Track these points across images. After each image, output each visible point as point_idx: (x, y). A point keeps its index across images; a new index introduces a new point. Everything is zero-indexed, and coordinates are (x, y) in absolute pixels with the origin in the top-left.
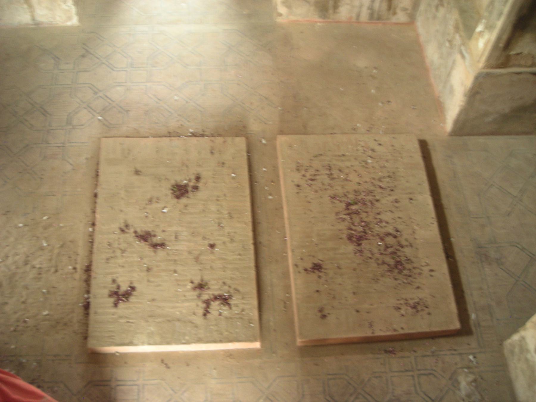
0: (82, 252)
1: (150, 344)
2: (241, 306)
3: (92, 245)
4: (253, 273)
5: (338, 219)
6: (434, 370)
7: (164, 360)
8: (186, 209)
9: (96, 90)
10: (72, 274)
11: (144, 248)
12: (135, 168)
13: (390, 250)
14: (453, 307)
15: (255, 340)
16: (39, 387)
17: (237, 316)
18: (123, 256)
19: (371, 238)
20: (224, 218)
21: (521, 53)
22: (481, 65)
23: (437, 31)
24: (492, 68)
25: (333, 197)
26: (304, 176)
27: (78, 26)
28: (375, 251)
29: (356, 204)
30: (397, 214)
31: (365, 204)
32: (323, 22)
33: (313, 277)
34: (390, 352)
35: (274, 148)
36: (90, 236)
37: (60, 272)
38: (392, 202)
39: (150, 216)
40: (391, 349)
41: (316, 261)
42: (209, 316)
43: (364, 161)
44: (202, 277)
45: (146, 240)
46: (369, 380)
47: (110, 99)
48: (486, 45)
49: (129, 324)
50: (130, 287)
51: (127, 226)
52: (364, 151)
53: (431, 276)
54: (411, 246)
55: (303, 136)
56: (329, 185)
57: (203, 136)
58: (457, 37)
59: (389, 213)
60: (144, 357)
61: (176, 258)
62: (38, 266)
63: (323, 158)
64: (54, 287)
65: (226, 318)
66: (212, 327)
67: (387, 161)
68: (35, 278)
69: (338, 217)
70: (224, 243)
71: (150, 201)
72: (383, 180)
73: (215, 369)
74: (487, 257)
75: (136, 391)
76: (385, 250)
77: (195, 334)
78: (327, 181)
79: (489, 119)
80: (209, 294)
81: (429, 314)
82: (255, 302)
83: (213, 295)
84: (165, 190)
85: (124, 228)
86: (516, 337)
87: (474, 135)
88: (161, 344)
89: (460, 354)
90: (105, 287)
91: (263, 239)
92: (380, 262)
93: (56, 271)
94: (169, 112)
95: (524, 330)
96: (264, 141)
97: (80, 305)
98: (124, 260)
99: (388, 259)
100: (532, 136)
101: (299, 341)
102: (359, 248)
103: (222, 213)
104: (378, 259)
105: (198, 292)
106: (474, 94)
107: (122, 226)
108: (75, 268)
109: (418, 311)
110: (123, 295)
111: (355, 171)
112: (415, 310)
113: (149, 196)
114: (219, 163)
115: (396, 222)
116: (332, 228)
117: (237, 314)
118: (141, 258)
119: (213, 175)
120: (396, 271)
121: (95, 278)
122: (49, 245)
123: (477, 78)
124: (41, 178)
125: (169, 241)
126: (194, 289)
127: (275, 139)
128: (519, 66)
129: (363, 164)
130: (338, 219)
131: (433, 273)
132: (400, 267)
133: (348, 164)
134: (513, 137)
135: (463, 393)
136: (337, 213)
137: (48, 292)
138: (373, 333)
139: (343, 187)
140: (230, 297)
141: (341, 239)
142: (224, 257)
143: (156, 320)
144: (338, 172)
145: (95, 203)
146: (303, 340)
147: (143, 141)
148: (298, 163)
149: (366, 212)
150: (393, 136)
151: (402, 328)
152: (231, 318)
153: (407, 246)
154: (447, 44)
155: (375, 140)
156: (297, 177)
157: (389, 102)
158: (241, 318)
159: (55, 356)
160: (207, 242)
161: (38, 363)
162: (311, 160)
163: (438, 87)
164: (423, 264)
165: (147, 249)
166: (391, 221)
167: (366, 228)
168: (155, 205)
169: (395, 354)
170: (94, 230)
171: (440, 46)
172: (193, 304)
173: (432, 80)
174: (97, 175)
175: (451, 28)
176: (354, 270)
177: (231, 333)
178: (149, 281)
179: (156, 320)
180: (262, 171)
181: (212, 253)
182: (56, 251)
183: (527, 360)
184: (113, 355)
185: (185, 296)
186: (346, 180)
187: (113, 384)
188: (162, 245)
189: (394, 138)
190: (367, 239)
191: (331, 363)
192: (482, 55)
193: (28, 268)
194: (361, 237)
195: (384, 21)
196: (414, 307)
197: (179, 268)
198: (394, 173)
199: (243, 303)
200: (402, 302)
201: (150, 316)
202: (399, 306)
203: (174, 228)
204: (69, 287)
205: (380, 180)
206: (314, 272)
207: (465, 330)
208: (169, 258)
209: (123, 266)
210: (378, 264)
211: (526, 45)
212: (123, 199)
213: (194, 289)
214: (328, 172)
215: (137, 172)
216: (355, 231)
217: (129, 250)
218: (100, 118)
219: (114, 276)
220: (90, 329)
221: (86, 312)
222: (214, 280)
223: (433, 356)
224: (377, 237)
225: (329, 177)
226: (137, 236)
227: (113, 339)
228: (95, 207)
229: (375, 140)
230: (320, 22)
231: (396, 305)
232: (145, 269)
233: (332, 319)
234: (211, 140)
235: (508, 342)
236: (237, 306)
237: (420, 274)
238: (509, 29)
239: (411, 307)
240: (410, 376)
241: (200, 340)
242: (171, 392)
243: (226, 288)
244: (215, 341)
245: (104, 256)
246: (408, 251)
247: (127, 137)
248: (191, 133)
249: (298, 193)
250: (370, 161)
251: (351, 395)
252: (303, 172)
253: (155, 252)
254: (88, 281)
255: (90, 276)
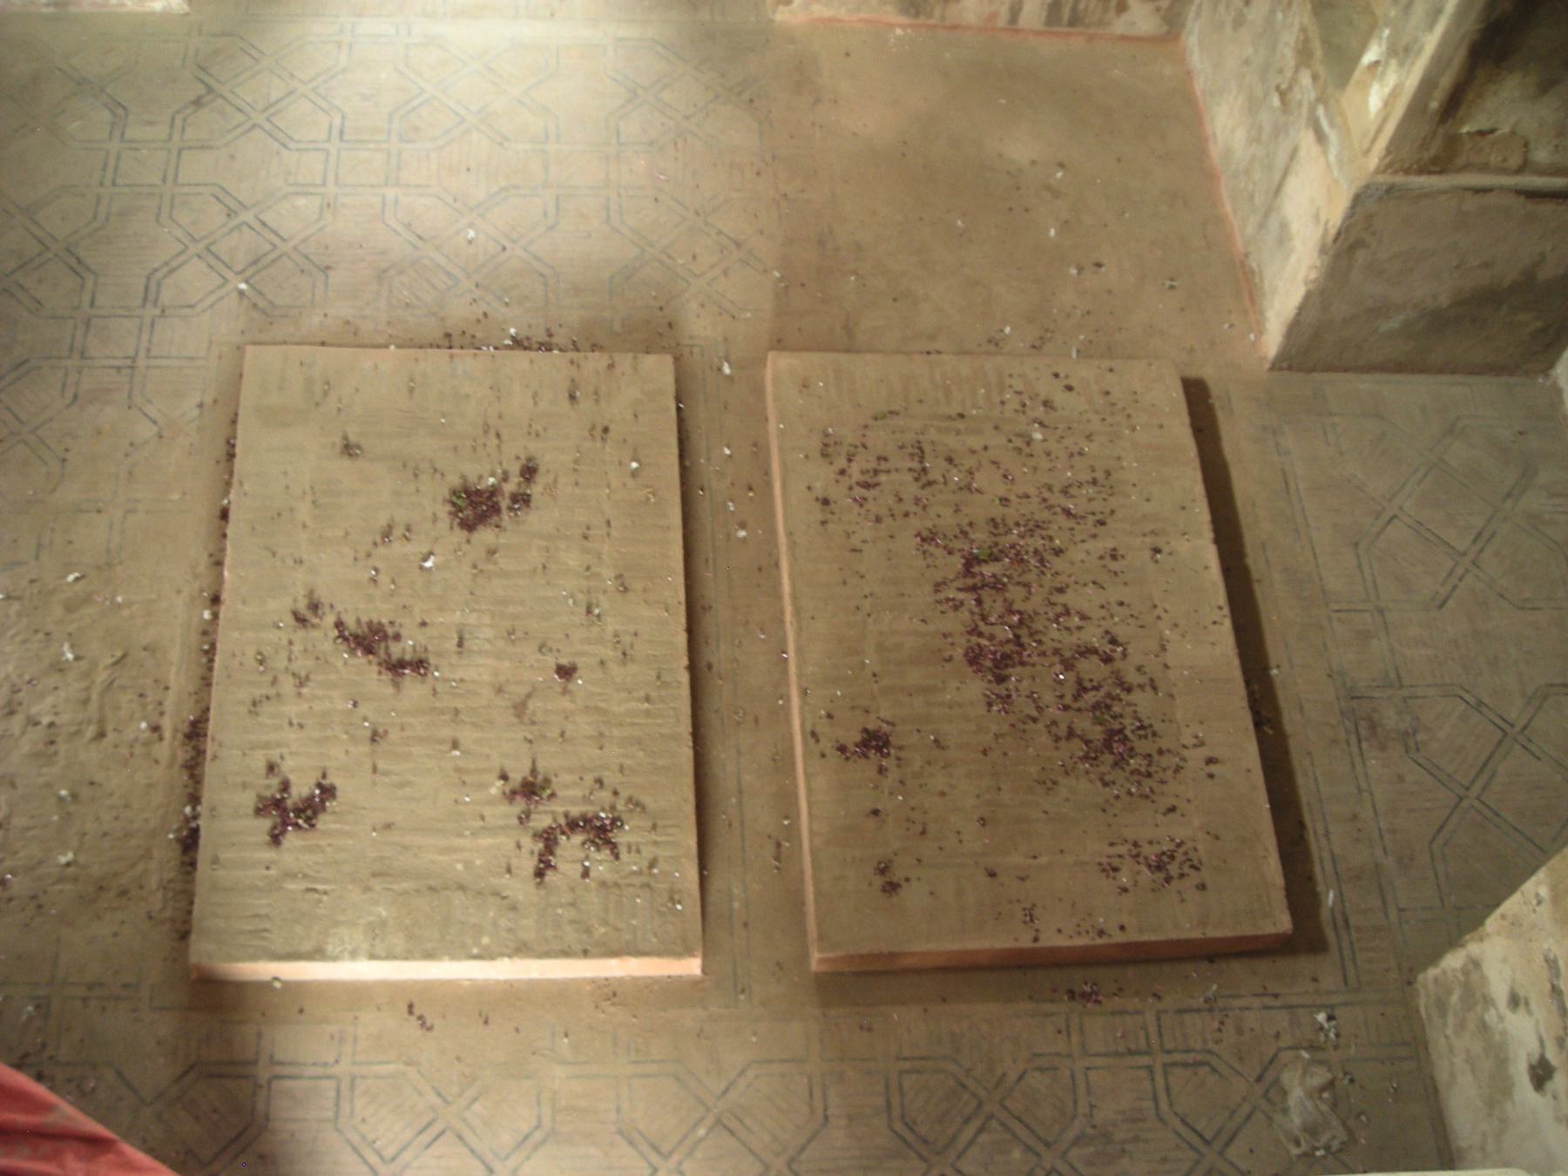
0: (178, 676)
1: (373, 956)
2: (648, 853)
3: (211, 660)
4: (686, 753)
5: (940, 602)
6: (1210, 1052)
7: (415, 1005)
8: (495, 563)
9: (232, 204)
10: (147, 744)
11: (366, 672)
12: (345, 438)
13: (1090, 698)
14: (1273, 866)
15: (688, 952)
16: (39, 1077)
17: (637, 881)
18: (299, 694)
19: (1035, 659)
20: (605, 592)
21: (1492, 131)
22: (1373, 162)
23: (1247, 62)
24: (1407, 172)
25: (928, 538)
26: (842, 472)
27: (187, 14)
28: (1048, 698)
29: (997, 560)
30: (1114, 593)
31: (1019, 560)
32: (914, 27)
33: (863, 769)
34: (1084, 996)
35: (758, 391)
36: (205, 633)
37: (111, 736)
38: (1101, 558)
39: (384, 579)
40: (1088, 989)
41: (870, 727)
42: (550, 876)
43: (1019, 435)
44: (534, 763)
45: (369, 651)
46: (1021, 1078)
47: (276, 233)
48: (1388, 103)
49: (309, 896)
50: (319, 785)
51: (315, 607)
52: (1024, 405)
53: (1211, 776)
54: (1155, 688)
55: (843, 358)
56: (917, 501)
57: (547, 347)
58: (1305, 79)
59: (1090, 589)
60: (356, 995)
61: (459, 704)
62: (45, 720)
63: (899, 421)
64: (92, 783)
65: (603, 884)
66: (560, 911)
67: (1089, 437)
68: (36, 755)
69: (941, 596)
70: (602, 663)
71: (387, 534)
72: (1073, 491)
73: (566, 1035)
74: (1373, 727)
75: (333, 1094)
76: (1076, 697)
77: (510, 930)
78: (911, 489)
79: (1394, 323)
80: (553, 813)
81: (1202, 887)
82: (692, 842)
83: (566, 815)
84: (432, 502)
85: (308, 615)
86: (1453, 961)
87: (1346, 370)
88: (407, 956)
89: (1289, 1007)
90: (245, 786)
91: (718, 654)
92: (1062, 730)
93: (101, 735)
94: (448, 273)
95: (1481, 939)
96: (727, 370)
97: (171, 836)
98: (305, 706)
99: (1083, 724)
100: (1512, 380)
101: (816, 959)
102: (1001, 689)
103: (598, 575)
104: (1054, 723)
105: (520, 805)
106: (1346, 247)
107: (302, 605)
108: (156, 729)
109: (1168, 879)
110: (299, 811)
111: (994, 462)
112: (1161, 875)
113: (382, 520)
114: (593, 428)
115: (1112, 616)
116: (922, 627)
117: (634, 873)
118: (355, 705)
119: (576, 462)
120: (1108, 758)
121: (215, 757)
122: (77, 658)
123: (1357, 200)
124: (64, 460)
125: (439, 654)
126: (511, 796)
127: (761, 362)
128: (1484, 168)
129: (1019, 442)
130: (940, 602)
131: (1213, 768)
132: (1119, 748)
133: (975, 442)
134: (1458, 378)
135: (1296, 1120)
136: (938, 586)
137: (75, 796)
138: (1036, 940)
139: (957, 511)
140: (616, 822)
141: (950, 659)
142: (601, 705)
143: (395, 887)
144: (945, 464)
145: (224, 536)
146: (831, 955)
147: (367, 360)
148: (827, 435)
149: (1027, 585)
150: (1107, 364)
151: (1122, 928)
152: (616, 885)
153: (1141, 686)
154: (1276, 101)
155: (1056, 375)
156: (822, 477)
157: (1099, 265)
158: (647, 886)
159: (90, 987)
160: (550, 661)
161: (38, 1007)
162: (866, 427)
163: (1242, 227)
164: (1190, 741)
165: (375, 676)
166: (1096, 613)
167: (1023, 632)
168: (398, 548)
169: (1098, 1002)
170: (215, 616)
171: (1253, 106)
172: (506, 842)
173: (1228, 208)
174: (231, 456)
175: (1287, 52)
176: (985, 752)
177: (617, 929)
178: (375, 770)
179: (395, 887)
180: (719, 456)
181: (565, 691)
182: (101, 677)
183: (1484, 1027)
184: (264, 987)
185: (483, 818)
186: (968, 488)
187: (263, 1075)
188: (419, 665)
189: (1111, 370)
190: (1023, 664)
191: (909, 1025)
192: (1379, 130)
193: (17, 722)
194: (1005, 656)
195: (1093, 30)
196: (1160, 867)
197: (466, 735)
198: (1108, 473)
199: (656, 843)
200: (1123, 849)
201: (374, 875)
202: (1116, 862)
203: (457, 617)
204: (141, 784)
205: (1065, 491)
206: (866, 757)
207: (1305, 938)
208: (438, 704)
209: (301, 726)
210: (1057, 739)
211: (1509, 108)
212: (304, 526)
213: (511, 796)
214: (915, 465)
215: (349, 449)
216: (991, 638)
217: (320, 678)
218: (243, 286)
219: (274, 755)
220: (197, 909)
221: (187, 859)
222: (570, 771)
223: (1211, 1010)
224: (1056, 659)
225: (916, 480)
226: (346, 639)
227: (264, 939)
228: (223, 550)
229: (1056, 375)
230: (902, 27)
231: (1104, 860)
232: (368, 734)
233: (913, 896)
234: (572, 362)
235: (1432, 972)
236: (635, 849)
237: (1178, 769)
238: (1462, 53)
239: (1149, 867)
240: (1140, 1067)
241: (522, 949)
242: (433, 1098)
243: (605, 795)
244: (566, 953)
245: (244, 694)
246: (1143, 701)
247: (323, 344)
248: (513, 339)
249: (824, 523)
250: (1038, 436)
251: (967, 1120)
252: (841, 462)
253: (397, 685)
254: (194, 768)
255: (200, 752)
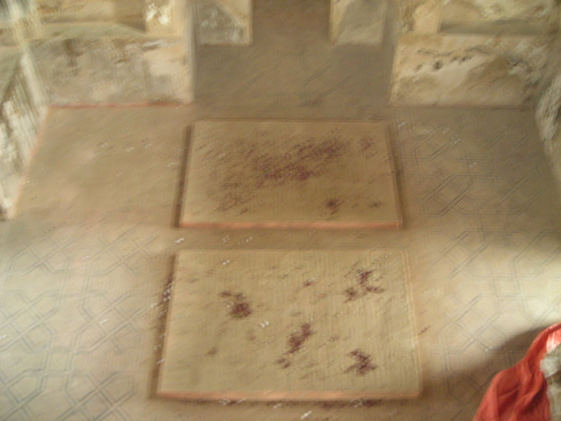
11: (308, 345)
183: (417, 83)
215: (213, 352)
235: (393, 99)
